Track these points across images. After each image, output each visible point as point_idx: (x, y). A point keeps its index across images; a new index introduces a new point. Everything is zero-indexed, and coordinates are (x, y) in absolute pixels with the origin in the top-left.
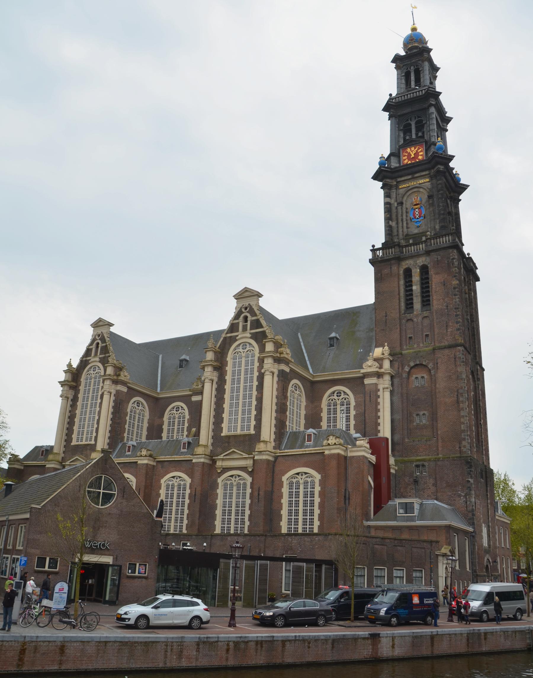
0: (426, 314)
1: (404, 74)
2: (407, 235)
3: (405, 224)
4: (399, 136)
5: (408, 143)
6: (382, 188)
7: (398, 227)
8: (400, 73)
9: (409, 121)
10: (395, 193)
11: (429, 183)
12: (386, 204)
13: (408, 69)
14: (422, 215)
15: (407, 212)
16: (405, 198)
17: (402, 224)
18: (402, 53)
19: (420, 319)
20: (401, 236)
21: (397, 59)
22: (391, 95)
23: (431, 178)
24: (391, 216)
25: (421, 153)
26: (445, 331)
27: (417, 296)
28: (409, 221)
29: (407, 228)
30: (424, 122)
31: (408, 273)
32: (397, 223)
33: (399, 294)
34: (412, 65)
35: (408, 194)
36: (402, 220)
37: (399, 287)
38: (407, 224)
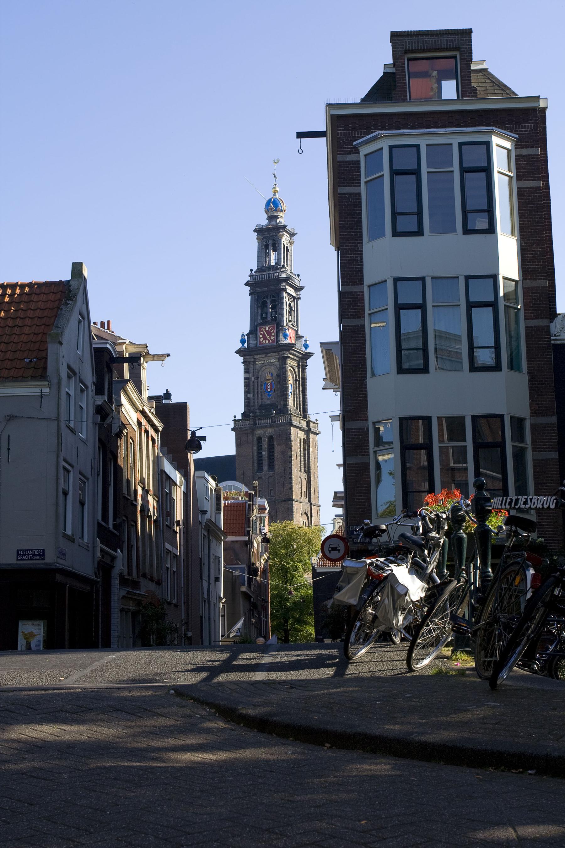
0: (271, 474)
1: (263, 247)
2: (261, 405)
3: (260, 396)
4: (257, 312)
5: (265, 322)
6: (242, 363)
7: (254, 399)
8: (261, 246)
9: (266, 299)
10: (252, 368)
11: (278, 363)
12: (245, 379)
13: (266, 242)
14: (273, 390)
15: (261, 385)
16: (260, 373)
17: (258, 396)
18: (263, 221)
19: (267, 477)
20: (256, 407)
21: (259, 231)
22: (251, 270)
23: (279, 359)
24: (249, 389)
25: (273, 334)
26: (283, 489)
27: (265, 460)
28: (263, 394)
29: (262, 399)
30: (277, 303)
31: (259, 439)
32: (254, 396)
33: (253, 458)
34: (270, 239)
35: (262, 369)
36: (258, 393)
37: (253, 452)
38: (261, 395)
